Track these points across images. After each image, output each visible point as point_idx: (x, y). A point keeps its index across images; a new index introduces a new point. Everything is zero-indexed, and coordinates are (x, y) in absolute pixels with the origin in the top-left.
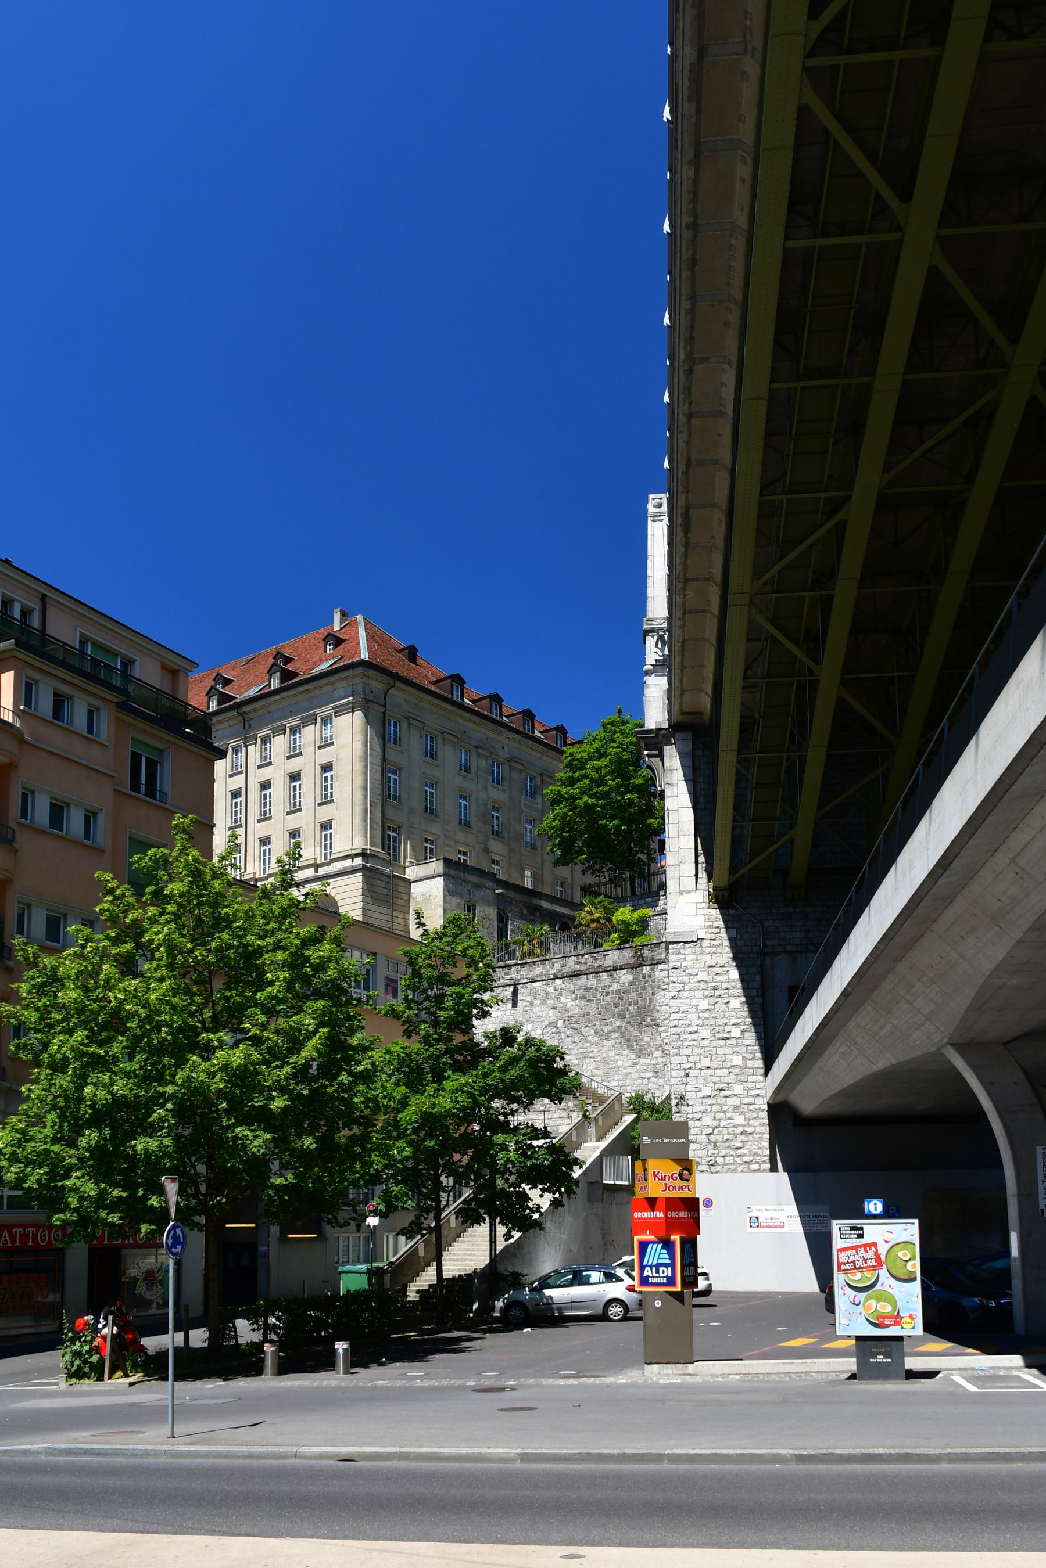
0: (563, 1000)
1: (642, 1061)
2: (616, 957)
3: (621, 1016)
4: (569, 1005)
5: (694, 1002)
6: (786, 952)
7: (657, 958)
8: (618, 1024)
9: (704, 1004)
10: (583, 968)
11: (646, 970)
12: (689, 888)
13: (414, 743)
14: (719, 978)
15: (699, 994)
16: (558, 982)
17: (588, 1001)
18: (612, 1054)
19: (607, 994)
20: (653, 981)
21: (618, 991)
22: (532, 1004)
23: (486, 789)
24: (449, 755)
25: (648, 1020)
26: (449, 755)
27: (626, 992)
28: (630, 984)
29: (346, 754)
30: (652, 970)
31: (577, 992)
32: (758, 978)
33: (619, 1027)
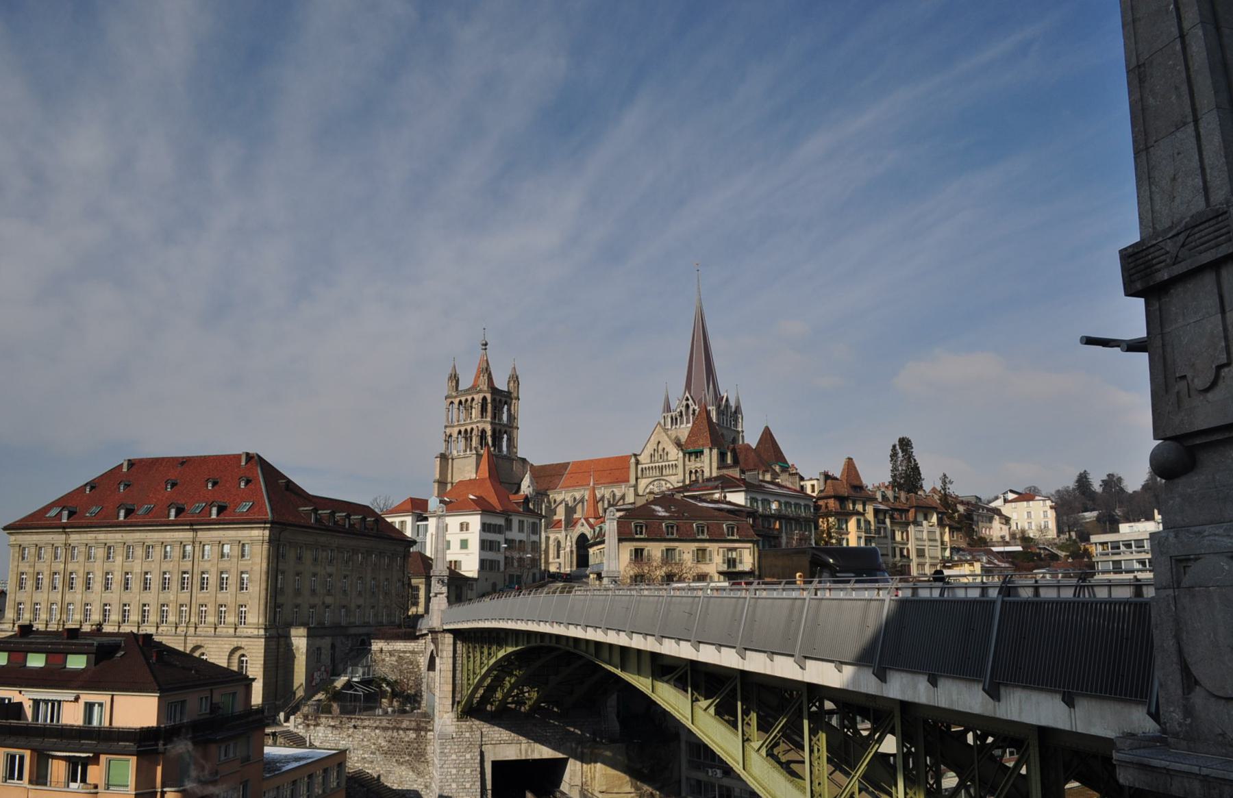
0: (379, 741)
1: (419, 780)
3: (411, 755)
4: (382, 744)
5: (449, 770)
6: (491, 744)
7: (429, 728)
8: (407, 758)
9: (454, 771)
10: (391, 726)
11: (423, 733)
12: (448, 711)
13: (291, 555)
14: (461, 758)
15: (451, 766)
16: (377, 731)
18: (404, 773)
19: (403, 742)
20: (426, 740)
21: (408, 742)
22: (363, 740)
23: (325, 568)
24: (308, 555)
25: (423, 759)
26: (308, 555)
27: (412, 742)
28: (415, 739)
29: (257, 568)
30: (426, 734)
31: (387, 738)
32: (479, 758)
33: (408, 760)
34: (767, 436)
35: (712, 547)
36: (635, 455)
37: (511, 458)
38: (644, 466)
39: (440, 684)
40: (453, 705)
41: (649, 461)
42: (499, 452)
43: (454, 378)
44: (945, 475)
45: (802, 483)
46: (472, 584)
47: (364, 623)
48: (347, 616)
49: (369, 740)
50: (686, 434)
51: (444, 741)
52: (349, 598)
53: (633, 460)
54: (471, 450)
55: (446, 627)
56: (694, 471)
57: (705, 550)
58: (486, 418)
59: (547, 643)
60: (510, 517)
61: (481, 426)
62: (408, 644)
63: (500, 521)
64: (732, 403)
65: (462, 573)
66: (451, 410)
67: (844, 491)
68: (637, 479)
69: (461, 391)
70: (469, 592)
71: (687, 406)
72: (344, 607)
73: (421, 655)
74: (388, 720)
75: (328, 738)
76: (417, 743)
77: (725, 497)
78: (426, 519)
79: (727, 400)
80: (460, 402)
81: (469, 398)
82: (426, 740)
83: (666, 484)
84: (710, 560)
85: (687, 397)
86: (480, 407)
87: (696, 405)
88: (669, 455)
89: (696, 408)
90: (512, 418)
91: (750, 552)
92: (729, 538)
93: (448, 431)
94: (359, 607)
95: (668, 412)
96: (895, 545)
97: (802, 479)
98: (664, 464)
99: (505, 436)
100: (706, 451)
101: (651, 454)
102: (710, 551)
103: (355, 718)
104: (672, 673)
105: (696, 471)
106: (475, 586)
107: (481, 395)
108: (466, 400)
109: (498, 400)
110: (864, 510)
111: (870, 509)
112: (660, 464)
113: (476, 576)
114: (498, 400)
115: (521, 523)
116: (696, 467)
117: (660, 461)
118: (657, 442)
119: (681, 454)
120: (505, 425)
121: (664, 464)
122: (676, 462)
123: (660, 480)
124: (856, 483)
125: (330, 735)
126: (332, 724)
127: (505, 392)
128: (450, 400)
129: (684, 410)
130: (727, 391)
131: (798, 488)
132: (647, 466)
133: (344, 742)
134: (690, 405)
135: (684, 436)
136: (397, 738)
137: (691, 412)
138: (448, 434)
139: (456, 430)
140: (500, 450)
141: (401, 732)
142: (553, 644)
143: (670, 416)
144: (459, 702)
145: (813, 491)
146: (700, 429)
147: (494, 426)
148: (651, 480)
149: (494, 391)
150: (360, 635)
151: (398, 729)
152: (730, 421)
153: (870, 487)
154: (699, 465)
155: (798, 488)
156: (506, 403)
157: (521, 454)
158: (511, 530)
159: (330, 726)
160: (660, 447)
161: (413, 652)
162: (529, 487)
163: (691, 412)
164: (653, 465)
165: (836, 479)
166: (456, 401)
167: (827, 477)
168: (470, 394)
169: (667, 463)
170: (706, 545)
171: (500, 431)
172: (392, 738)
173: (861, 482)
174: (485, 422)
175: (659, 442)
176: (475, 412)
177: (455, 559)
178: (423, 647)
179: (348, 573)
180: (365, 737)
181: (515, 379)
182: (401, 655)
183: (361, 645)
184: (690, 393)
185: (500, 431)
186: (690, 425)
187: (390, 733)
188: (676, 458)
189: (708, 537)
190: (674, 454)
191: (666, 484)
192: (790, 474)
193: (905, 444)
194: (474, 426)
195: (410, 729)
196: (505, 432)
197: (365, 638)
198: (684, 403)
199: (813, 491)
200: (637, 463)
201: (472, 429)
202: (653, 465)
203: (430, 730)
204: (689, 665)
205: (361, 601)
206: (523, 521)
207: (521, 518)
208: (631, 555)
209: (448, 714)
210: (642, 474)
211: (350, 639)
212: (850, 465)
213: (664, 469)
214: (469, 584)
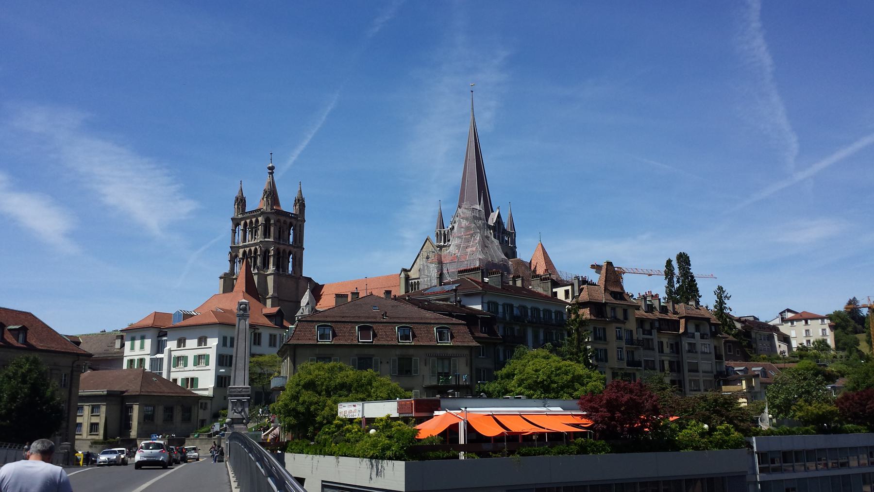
36: (405, 270)
42: (282, 271)
43: (241, 202)
46: (206, 404)
53: (403, 275)
57: (371, 359)
67: (602, 297)
70: (201, 411)
77: (460, 302)
78: (165, 335)
80: (245, 224)
84: (416, 372)
90: (299, 238)
91: (467, 361)
106: (209, 406)
109: (282, 221)
110: (626, 318)
114: (282, 221)
120: (292, 245)
127: (292, 214)
131: (550, 294)
138: (234, 254)
139: (241, 251)
143: (442, 232)
147: (278, 246)
153: (636, 296)
155: (550, 294)
158: (259, 344)
162: (308, 304)
165: (594, 285)
166: (243, 222)
168: (254, 216)
170: (411, 352)
171: (284, 250)
173: (622, 288)
177: (192, 376)
181: (300, 203)
192: (541, 280)
193: (683, 259)
200: (407, 278)
206: (275, 336)
214: (201, 403)
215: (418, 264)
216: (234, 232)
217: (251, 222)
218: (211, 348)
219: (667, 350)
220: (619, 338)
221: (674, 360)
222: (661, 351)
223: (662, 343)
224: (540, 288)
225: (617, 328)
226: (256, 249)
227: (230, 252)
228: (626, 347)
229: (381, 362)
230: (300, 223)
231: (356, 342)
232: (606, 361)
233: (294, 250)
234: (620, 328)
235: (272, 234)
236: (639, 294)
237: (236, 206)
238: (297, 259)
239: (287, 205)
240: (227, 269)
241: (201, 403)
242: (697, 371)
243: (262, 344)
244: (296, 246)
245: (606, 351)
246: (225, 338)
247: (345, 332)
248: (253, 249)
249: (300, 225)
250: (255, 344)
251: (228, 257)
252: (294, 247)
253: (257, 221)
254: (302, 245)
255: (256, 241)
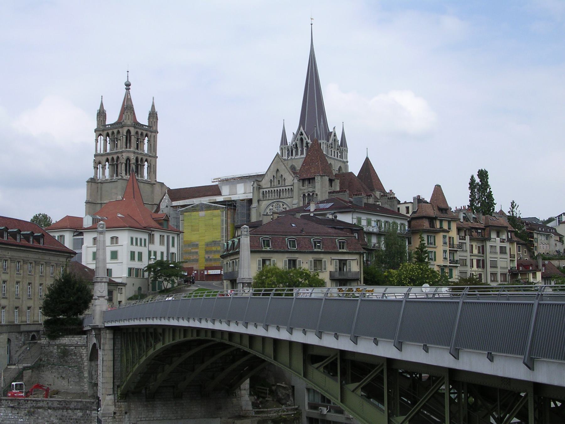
0: (52, 419)
2: (75, 405)
4: (54, 421)
16: (49, 411)
17: (63, 421)
19: (71, 419)
20: (91, 417)
21: (76, 419)
22: (38, 418)
28: (82, 417)
30: (91, 413)
31: (58, 417)
34: (367, 166)
35: (326, 258)
37: (153, 183)
38: (264, 190)
39: (103, 371)
40: (113, 388)
41: (269, 186)
43: (101, 114)
44: (513, 201)
45: (398, 206)
47: (34, 321)
48: (19, 316)
49: (43, 418)
50: (301, 162)
51: (107, 418)
52: (21, 302)
54: (117, 176)
55: (106, 325)
56: (306, 195)
58: (130, 148)
59: (202, 337)
60: (153, 233)
61: (125, 155)
62: (73, 339)
63: (145, 236)
64: (339, 138)
65: (112, 279)
66: (99, 141)
67: (432, 212)
68: (259, 201)
69: (108, 125)
70: (119, 295)
71: (302, 140)
72: (17, 308)
73: (84, 348)
74: (59, 401)
75: (8, 417)
76: (84, 420)
77: (336, 217)
78: (81, 234)
79: (335, 135)
81: (115, 131)
82: (91, 417)
83: (283, 205)
84: (325, 269)
85: (301, 132)
86: (125, 139)
87: (309, 139)
88: (286, 181)
89: (309, 141)
90: (153, 147)
92: (340, 251)
93: (99, 158)
94: (29, 308)
95: (285, 144)
96: (472, 257)
97: (399, 202)
98: (281, 188)
99: (146, 163)
100: (318, 179)
101: (271, 180)
102: (325, 262)
103: (31, 400)
104: (322, 361)
105: (309, 194)
107: (125, 129)
108: (113, 133)
109: (140, 133)
110: (449, 228)
111: (454, 226)
112: (278, 189)
113: (124, 282)
114: (140, 133)
115: (162, 237)
116: (309, 191)
117: (280, 185)
118: (276, 170)
119: (296, 181)
120: (146, 155)
121: (281, 188)
122: (292, 187)
123: (277, 201)
124: (443, 206)
125: (10, 414)
126: (11, 405)
128: (99, 133)
129: (299, 143)
130: (334, 128)
131: (397, 211)
132: (267, 190)
133: (22, 420)
134: (304, 139)
135: (298, 165)
136: (67, 416)
137: (305, 144)
138: (97, 161)
139: (104, 158)
140: (142, 176)
141: (70, 411)
142: (209, 337)
144: (118, 386)
145: (408, 212)
146: (313, 159)
147: (136, 155)
148: (270, 202)
149: (137, 125)
150: (31, 332)
151: (67, 409)
152: (337, 153)
153: (453, 209)
154: (311, 190)
156: (147, 135)
157: (160, 178)
158: (153, 243)
159: (9, 407)
160: (279, 175)
161: (76, 346)
163: (305, 144)
164: (273, 189)
165: (426, 202)
166: (105, 133)
167: (419, 200)
169: (284, 188)
170: (322, 256)
172: (62, 416)
174: (128, 152)
175: (278, 170)
176: (121, 143)
178: (85, 341)
179: (19, 280)
180: (39, 416)
181: (153, 115)
182: (67, 348)
183: (32, 340)
184: (304, 129)
185: (142, 159)
186: (304, 156)
187: (60, 412)
188: (292, 184)
189: (323, 251)
190: (290, 179)
191: (283, 205)
193: (483, 175)
194: (120, 155)
195: (77, 409)
196: (146, 160)
197: (35, 334)
198: (299, 137)
199: (408, 212)
201: (118, 158)
202: (273, 189)
203: (94, 410)
204: (339, 354)
205: (31, 303)
207: (162, 234)
208: (259, 265)
209: (110, 396)
210: (263, 197)
211: (23, 335)
212: (438, 190)
213: (281, 194)
214: (119, 288)
215: (269, 175)
216: (97, 140)
217: (113, 133)
218: (122, 245)
219: (475, 251)
220: (445, 243)
221: (481, 258)
222: (472, 251)
223: (472, 245)
224: (388, 204)
225: (443, 236)
226: (118, 158)
227: (94, 160)
228: (449, 250)
229: (303, 263)
230: (153, 134)
231: (287, 250)
232: (435, 260)
233: (149, 159)
234: (446, 236)
235: (132, 145)
236: (456, 207)
237: (98, 119)
238: (152, 166)
239: (143, 118)
240: (92, 176)
241: (119, 288)
242: (496, 267)
243: (155, 243)
244: (150, 155)
245: (435, 252)
246: (132, 239)
247: (279, 242)
248: (115, 157)
249: (154, 136)
250: (150, 243)
251: (92, 164)
252: (150, 156)
253: (118, 132)
254: (156, 154)
255: (117, 151)
